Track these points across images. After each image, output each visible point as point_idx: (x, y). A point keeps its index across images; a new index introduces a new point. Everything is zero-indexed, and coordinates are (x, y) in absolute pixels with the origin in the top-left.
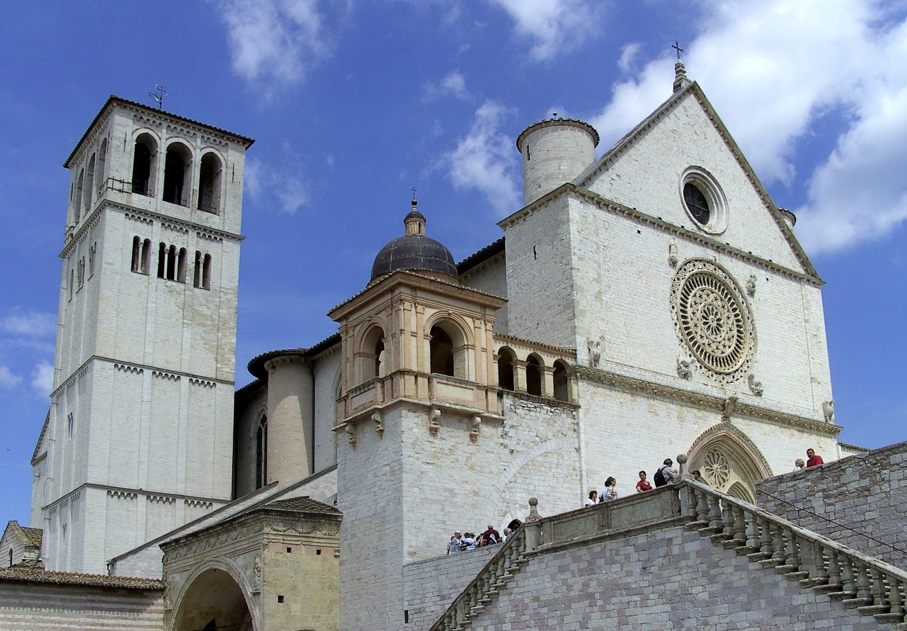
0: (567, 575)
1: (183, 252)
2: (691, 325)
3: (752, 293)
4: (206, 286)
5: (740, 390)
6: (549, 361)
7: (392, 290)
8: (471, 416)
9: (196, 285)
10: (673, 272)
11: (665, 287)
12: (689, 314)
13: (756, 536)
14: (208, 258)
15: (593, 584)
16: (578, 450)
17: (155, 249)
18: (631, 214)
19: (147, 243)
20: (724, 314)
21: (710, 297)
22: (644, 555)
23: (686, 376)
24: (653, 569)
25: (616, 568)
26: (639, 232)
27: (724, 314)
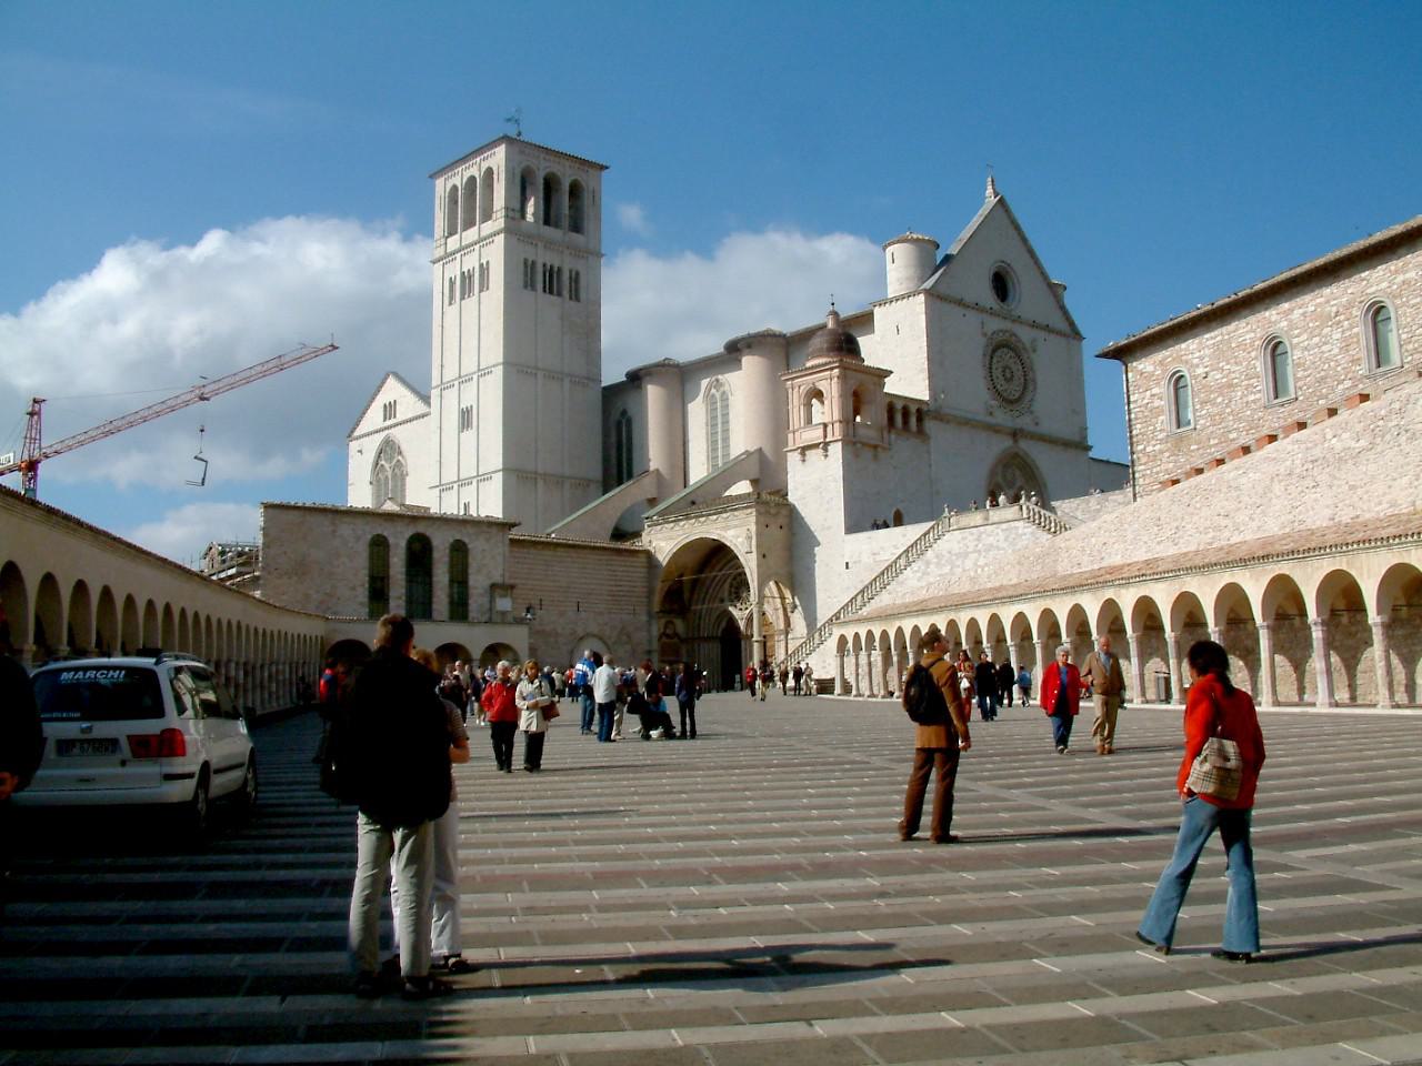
0: (967, 541)
1: (559, 269)
2: (994, 377)
3: (1034, 351)
4: (578, 299)
5: (1025, 422)
6: (913, 409)
7: (832, 369)
8: (875, 447)
9: (571, 298)
10: (983, 341)
11: (980, 352)
12: (994, 371)
13: (1056, 527)
14: (577, 274)
15: (980, 545)
16: (930, 466)
17: (540, 269)
18: (960, 303)
19: (533, 263)
20: (1017, 368)
21: (1006, 356)
22: (1007, 532)
23: (991, 414)
24: (1010, 540)
25: (991, 538)
26: (964, 315)
27: (1014, 368)
